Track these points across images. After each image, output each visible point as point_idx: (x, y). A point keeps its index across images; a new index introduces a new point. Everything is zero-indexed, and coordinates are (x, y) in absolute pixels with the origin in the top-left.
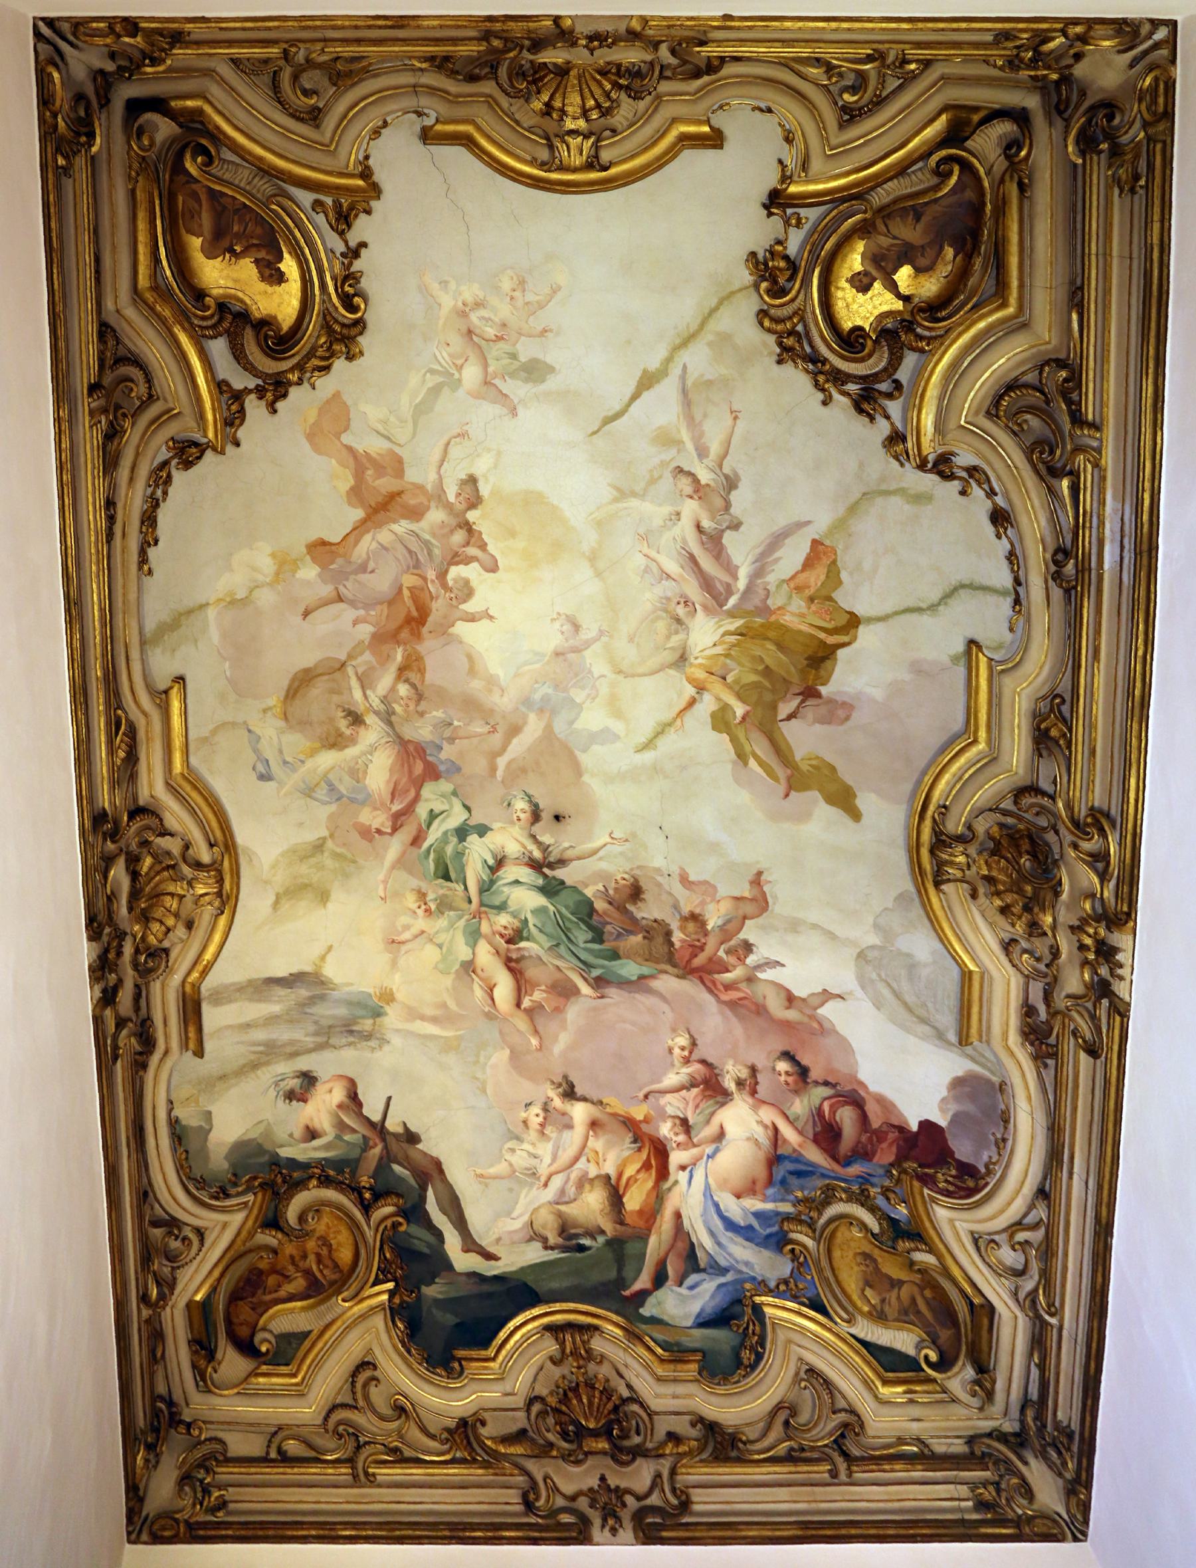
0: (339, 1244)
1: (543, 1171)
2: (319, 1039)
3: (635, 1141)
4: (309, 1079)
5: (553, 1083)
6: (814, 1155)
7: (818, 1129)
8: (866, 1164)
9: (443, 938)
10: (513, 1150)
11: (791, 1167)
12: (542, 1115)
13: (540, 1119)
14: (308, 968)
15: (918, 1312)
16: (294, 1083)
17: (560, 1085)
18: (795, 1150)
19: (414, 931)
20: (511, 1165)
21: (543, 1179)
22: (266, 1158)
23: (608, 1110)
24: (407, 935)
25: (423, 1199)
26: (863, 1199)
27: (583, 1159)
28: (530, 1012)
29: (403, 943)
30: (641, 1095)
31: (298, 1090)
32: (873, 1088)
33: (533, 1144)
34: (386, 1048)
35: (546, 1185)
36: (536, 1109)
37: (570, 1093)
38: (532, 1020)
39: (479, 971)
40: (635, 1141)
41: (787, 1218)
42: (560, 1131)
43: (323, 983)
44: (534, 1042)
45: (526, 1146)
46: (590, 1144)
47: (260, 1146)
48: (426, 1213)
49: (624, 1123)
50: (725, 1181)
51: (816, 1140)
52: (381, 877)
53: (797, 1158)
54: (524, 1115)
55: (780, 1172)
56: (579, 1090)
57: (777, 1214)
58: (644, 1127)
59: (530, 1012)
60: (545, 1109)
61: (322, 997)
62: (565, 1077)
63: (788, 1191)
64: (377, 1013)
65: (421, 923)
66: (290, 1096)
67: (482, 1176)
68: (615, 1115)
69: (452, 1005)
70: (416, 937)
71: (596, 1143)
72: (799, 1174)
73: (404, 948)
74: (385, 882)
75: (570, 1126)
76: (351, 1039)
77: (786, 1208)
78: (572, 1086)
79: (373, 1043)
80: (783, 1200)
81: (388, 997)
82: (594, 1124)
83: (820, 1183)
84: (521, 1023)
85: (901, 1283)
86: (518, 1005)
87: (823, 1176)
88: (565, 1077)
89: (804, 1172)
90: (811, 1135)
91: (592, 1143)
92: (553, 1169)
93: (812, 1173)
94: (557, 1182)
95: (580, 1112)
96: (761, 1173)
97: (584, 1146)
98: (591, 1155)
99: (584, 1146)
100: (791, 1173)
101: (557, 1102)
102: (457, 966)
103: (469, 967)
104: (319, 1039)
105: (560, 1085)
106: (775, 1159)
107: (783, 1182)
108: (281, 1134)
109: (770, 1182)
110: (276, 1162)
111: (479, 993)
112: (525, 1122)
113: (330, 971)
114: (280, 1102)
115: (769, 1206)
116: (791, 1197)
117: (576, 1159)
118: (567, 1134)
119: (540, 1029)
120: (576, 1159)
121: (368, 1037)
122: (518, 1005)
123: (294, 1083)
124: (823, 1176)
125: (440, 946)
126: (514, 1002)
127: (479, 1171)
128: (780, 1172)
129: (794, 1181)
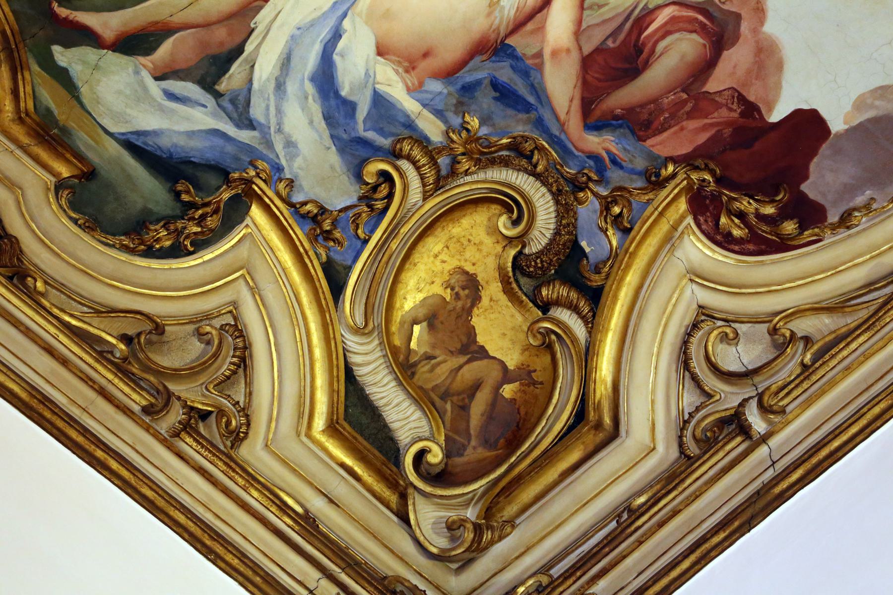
6: (561, 85)
7: (610, 44)
8: (630, 143)
11: (505, 73)
15: (464, 409)
18: (539, 55)
26: (567, 192)
32: (772, 27)
41: (422, 141)
50: (387, 15)
51: (586, 62)
53: (529, 70)
55: (480, 71)
57: (410, 124)
63: (461, 107)
72: (505, 95)
77: (432, 128)
80: (439, 114)
83: (520, 129)
85: (482, 353)
87: (539, 124)
89: (518, 94)
90: (587, 49)
93: (527, 108)
96: (451, 50)
100: (495, 85)
106: (494, 47)
107: (468, 89)
109: (448, 74)
115: (410, 105)
116: (456, 121)
124: (539, 124)
128: (480, 71)
129: (486, 99)
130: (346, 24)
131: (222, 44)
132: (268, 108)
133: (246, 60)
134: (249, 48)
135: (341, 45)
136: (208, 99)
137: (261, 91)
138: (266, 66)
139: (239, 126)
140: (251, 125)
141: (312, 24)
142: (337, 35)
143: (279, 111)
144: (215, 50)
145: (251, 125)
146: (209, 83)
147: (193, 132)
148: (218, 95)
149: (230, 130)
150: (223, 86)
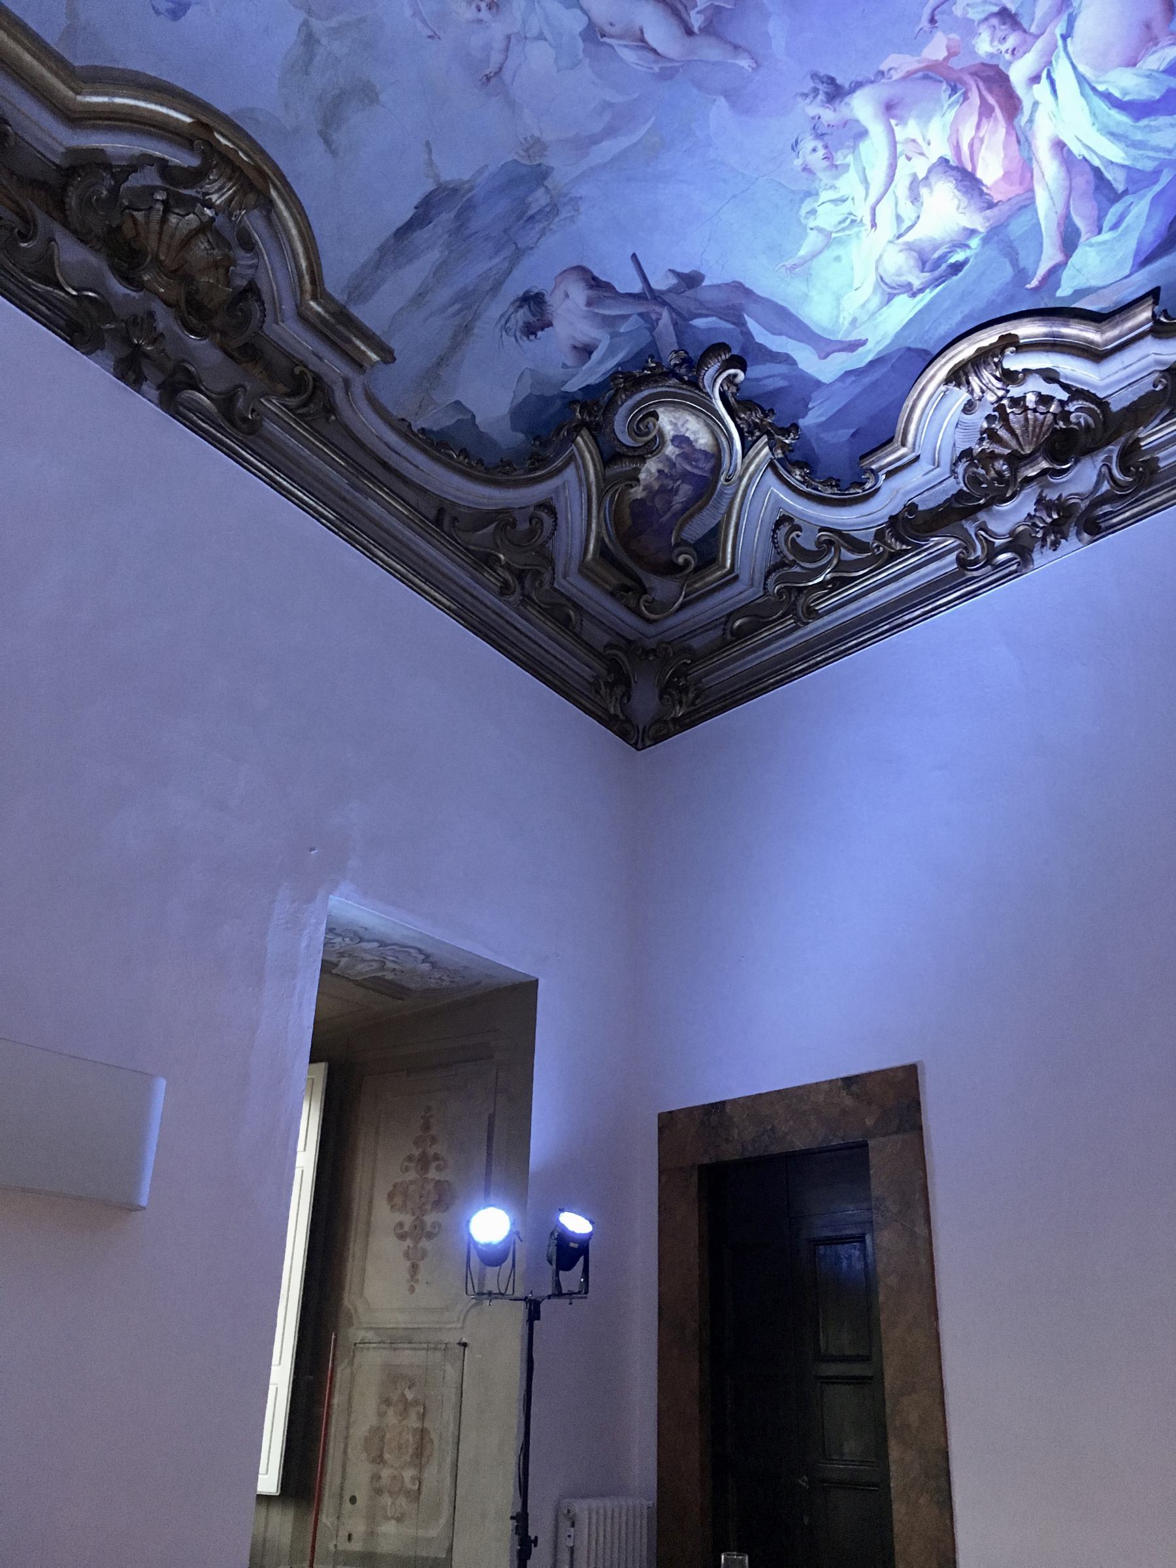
0: (694, 433)
1: (863, 212)
2: (508, 251)
3: (954, 90)
4: (534, 301)
5: (806, 95)
9: (535, 24)
10: (813, 212)
12: (819, 145)
13: (821, 152)
14: (430, 186)
16: (522, 315)
17: (816, 91)
19: (499, 44)
20: (820, 230)
21: (867, 220)
22: (558, 404)
23: (896, 76)
24: (496, 58)
25: (748, 335)
27: (902, 161)
28: (709, 29)
29: (500, 69)
30: (924, 23)
31: (532, 319)
33: (833, 187)
34: (583, 207)
35: (874, 225)
36: (809, 143)
37: (836, 92)
38: (719, 37)
39: (608, 29)
40: (954, 90)
42: (854, 148)
43: (455, 190)
44: (745, 63)
45: (825, 195)
46: (899, 137)
47: (541, 398)
48: (761, 347)
49: (926, 77)
52: (408, 12)
54: (798, 162)
56: (843, 80)
58: (955, 63)
59: (709, 29)
60: (820, 136)
61: (470, 206)
62: (814, 76)
64: (541, 175)
65: (498, 29)
66: (530, 330)
67: (794, 267)
68: (908, 76)
69: (611, 96)
70: (507, 49)
71: (908, 130)
73: (506, 76)
74: (416, 13)
75: (863, 134)
76: (538, 227)
78: (832, 81)
79: (565, 213)
81: (536, 145)
82: (890, 108)
84: (710, 51)
86: (689, 32)
88: (814, 76)
91: (901, 133)
92: (872, 199)
94: (885, 213)
95: (862, 107)
97: (894, 144)
98: (910, 149)
99: (894, 144)
101: (828, 115)
102: (580, 44)
103: (594, 34)
104: (508, 251)
105: (816, 91)
108: (554, 372)
110: (570, 400)
111: (629, 56)
112: (806, 169)
113: (453, 171)
114: (524, 342)
117: (893, 167)
118: (864, 147)
119: (738, 41)
120: (893, 167)
121: (553, 209)
122: (689, 32)
123: (522, 315)
125: (541, 37)
126: (678, 31)
127: (789, 263)
130: (1101, 88)
131: (1088, 182)
132: (1149, 157)
133: (1105, 167)
134: (1096, 162)
135: (1117, 94)
136: (1128, 199)
137: (1135, 159)
138: (1114, 152)
139: (1155, 182)
140: (1157, 173)
141: (1094, 114)
142: (1107, 97)
143: (1156, 149)
144: (1092, 187)
145: (1157, 173)
146: (1116, 197)
147: (1148, 216)
148: (1126, 192)
149: (1157, 188)
150: (1120, 187)
